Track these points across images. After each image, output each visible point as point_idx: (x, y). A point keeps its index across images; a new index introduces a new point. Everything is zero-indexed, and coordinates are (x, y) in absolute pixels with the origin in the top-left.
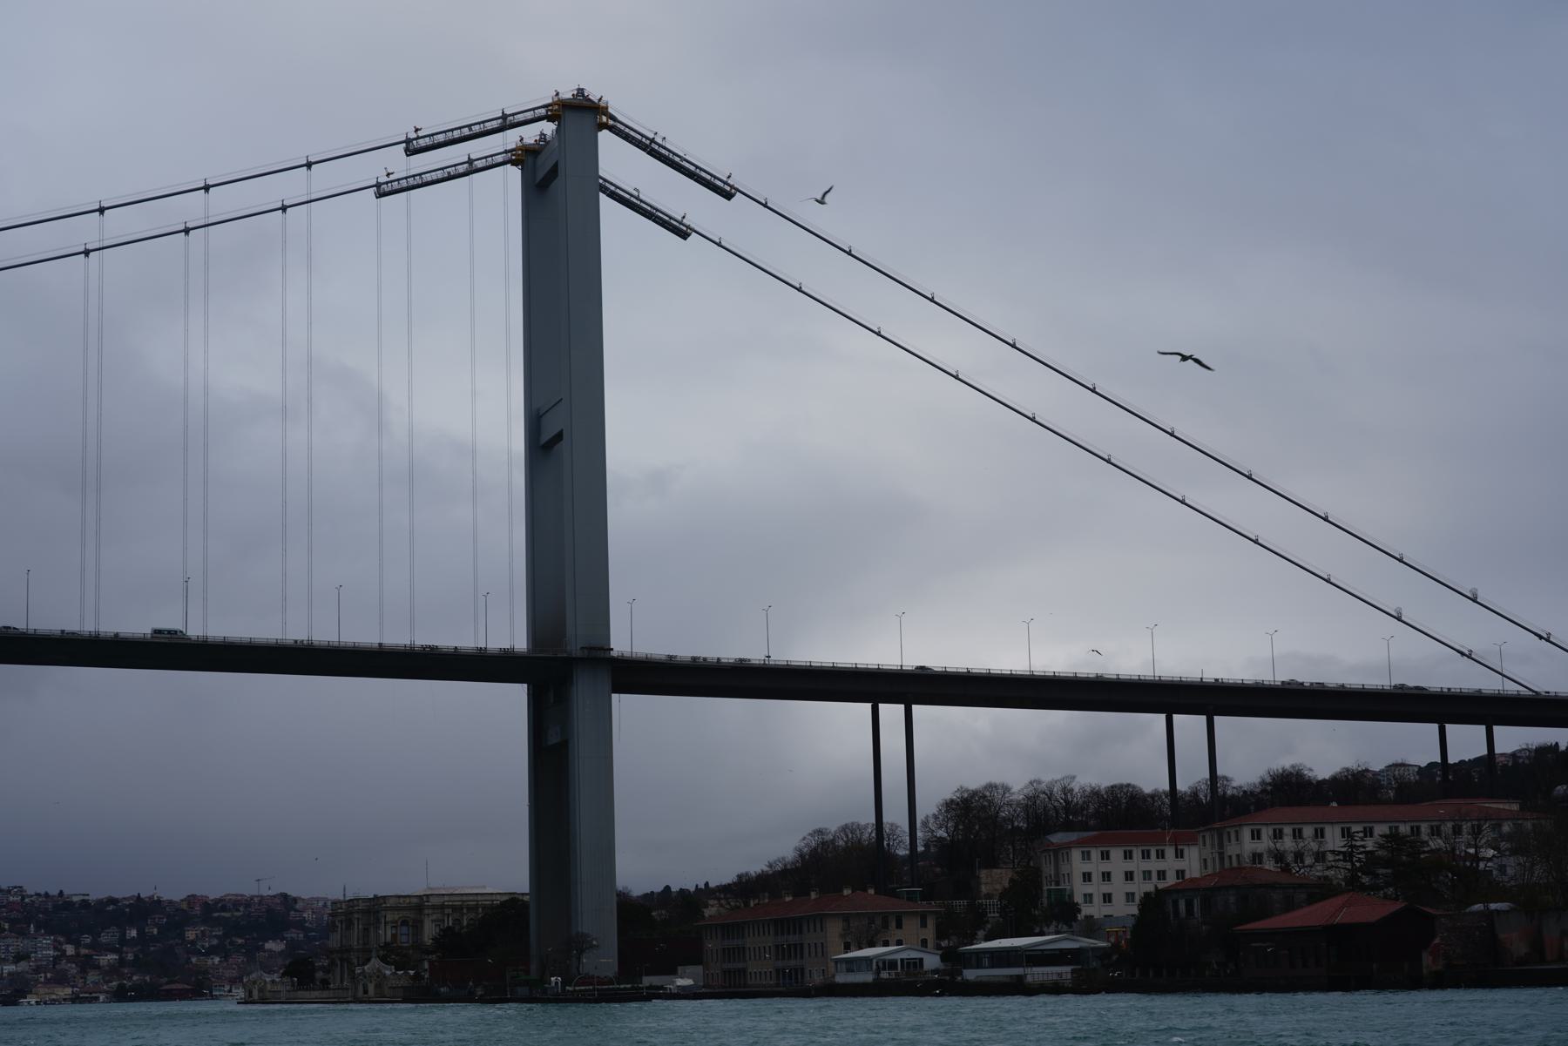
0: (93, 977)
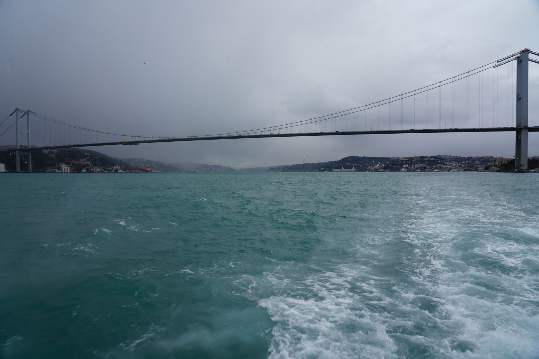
0: (461, 168)
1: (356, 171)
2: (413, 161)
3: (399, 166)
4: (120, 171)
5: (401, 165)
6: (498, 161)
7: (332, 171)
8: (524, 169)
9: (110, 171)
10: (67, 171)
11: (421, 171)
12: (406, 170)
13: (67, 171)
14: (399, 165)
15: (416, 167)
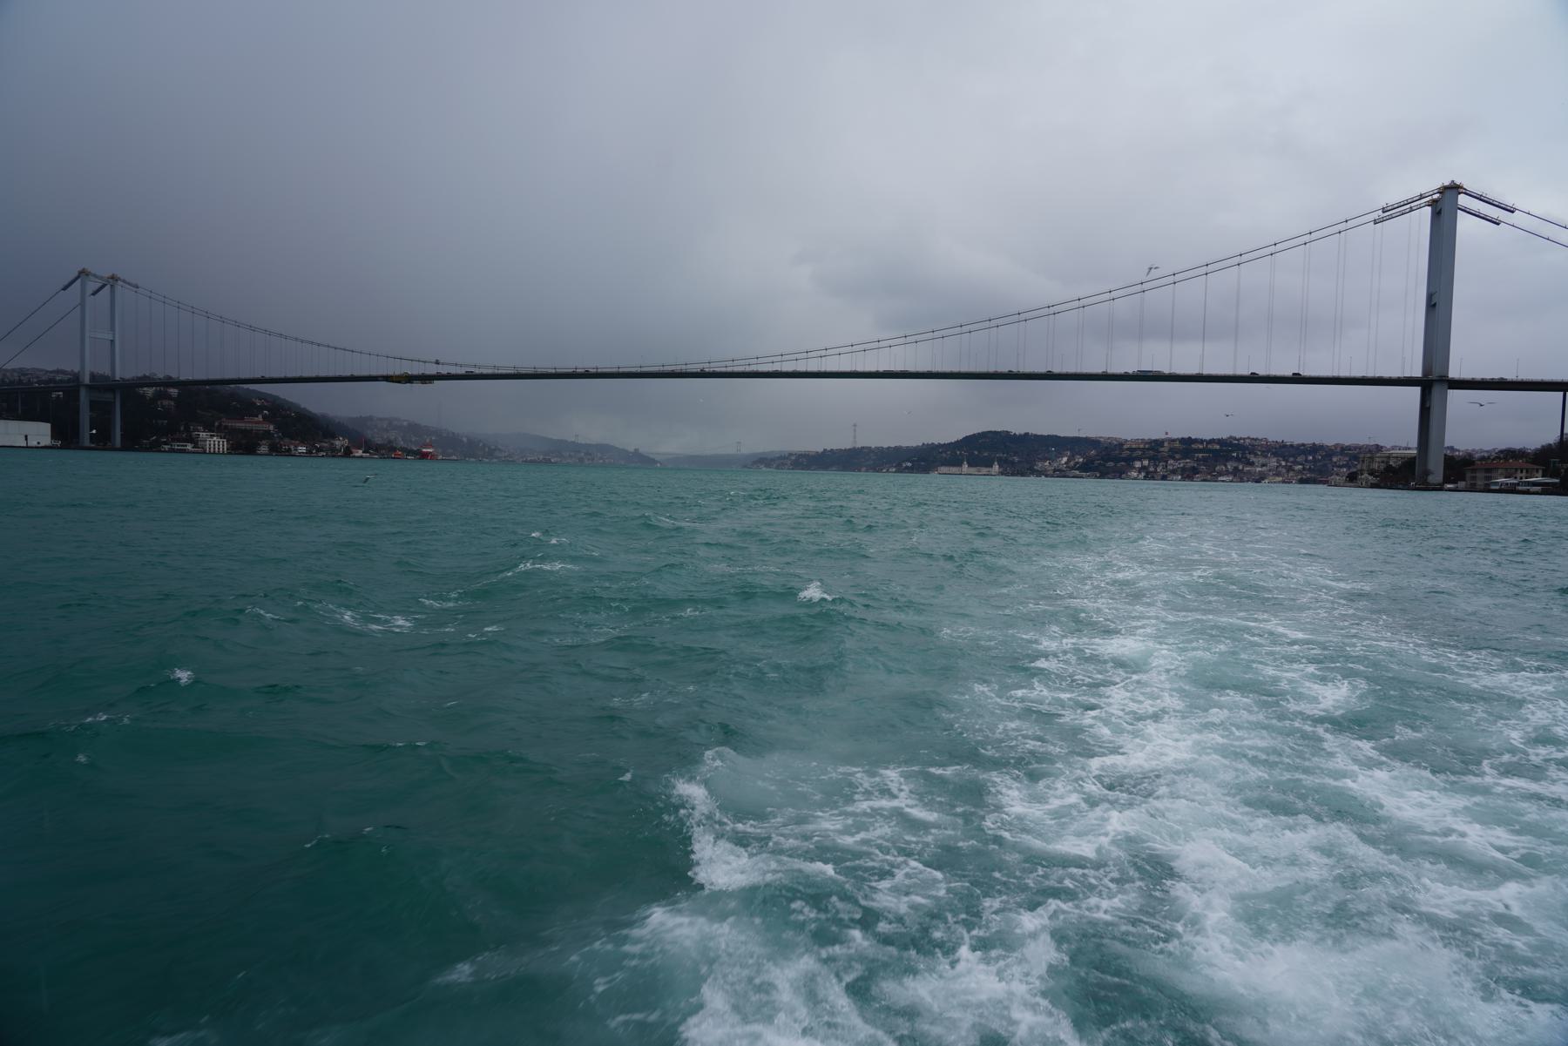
0: (1291, 474)
1: (1002, 474)
2: (1162, 449)
3: (1123, 463)
4: (356, 455)
5: (1129, 461)
6: (1377, 460)
8: (1431, 482)
9: (333, 453)
10: (217, 449)
11: (1183, 479)
12: (1143, 474)
13: (217, 449)
14: (1124, 460)
15: (1170, 467)
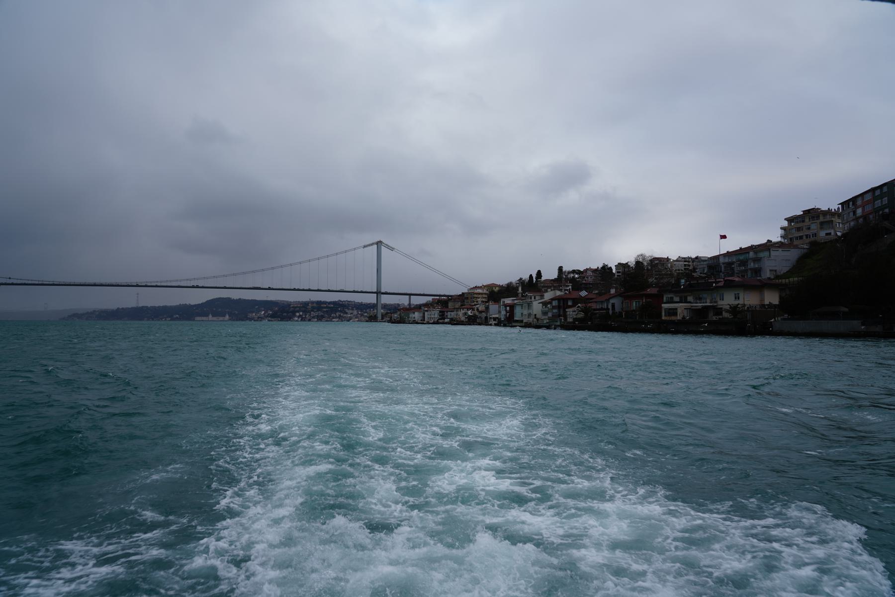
1: (230, 320)
5: (294, 313)
7: (194, 320)
